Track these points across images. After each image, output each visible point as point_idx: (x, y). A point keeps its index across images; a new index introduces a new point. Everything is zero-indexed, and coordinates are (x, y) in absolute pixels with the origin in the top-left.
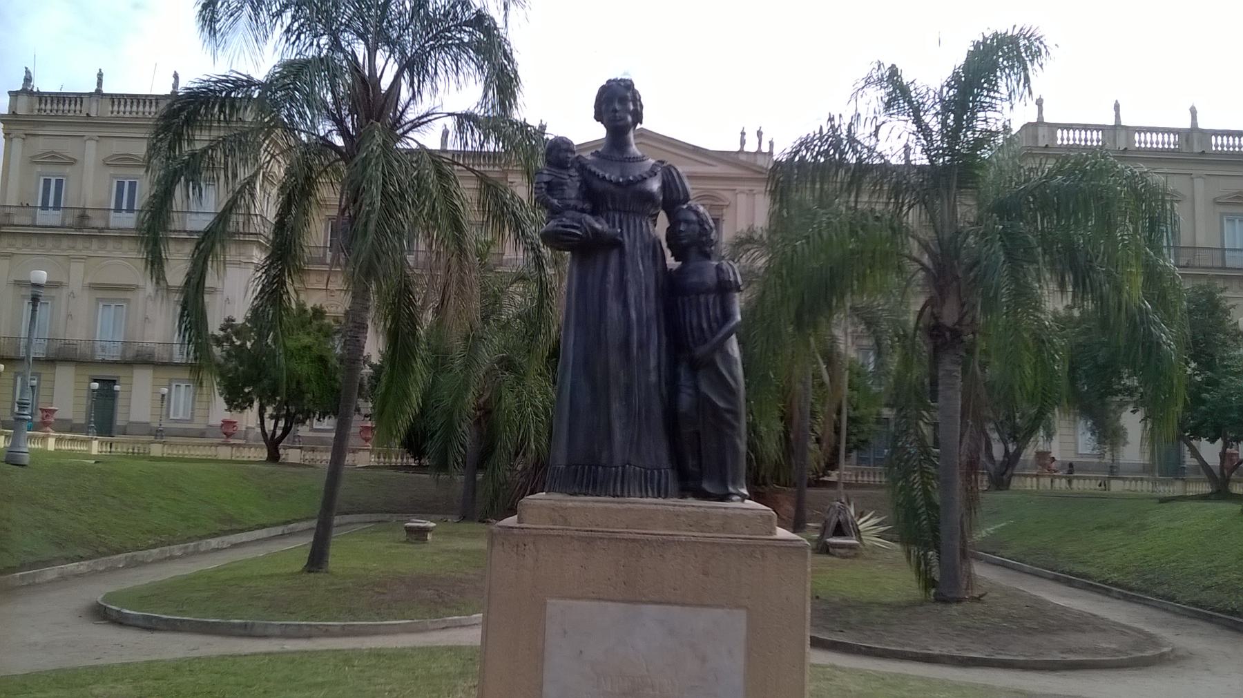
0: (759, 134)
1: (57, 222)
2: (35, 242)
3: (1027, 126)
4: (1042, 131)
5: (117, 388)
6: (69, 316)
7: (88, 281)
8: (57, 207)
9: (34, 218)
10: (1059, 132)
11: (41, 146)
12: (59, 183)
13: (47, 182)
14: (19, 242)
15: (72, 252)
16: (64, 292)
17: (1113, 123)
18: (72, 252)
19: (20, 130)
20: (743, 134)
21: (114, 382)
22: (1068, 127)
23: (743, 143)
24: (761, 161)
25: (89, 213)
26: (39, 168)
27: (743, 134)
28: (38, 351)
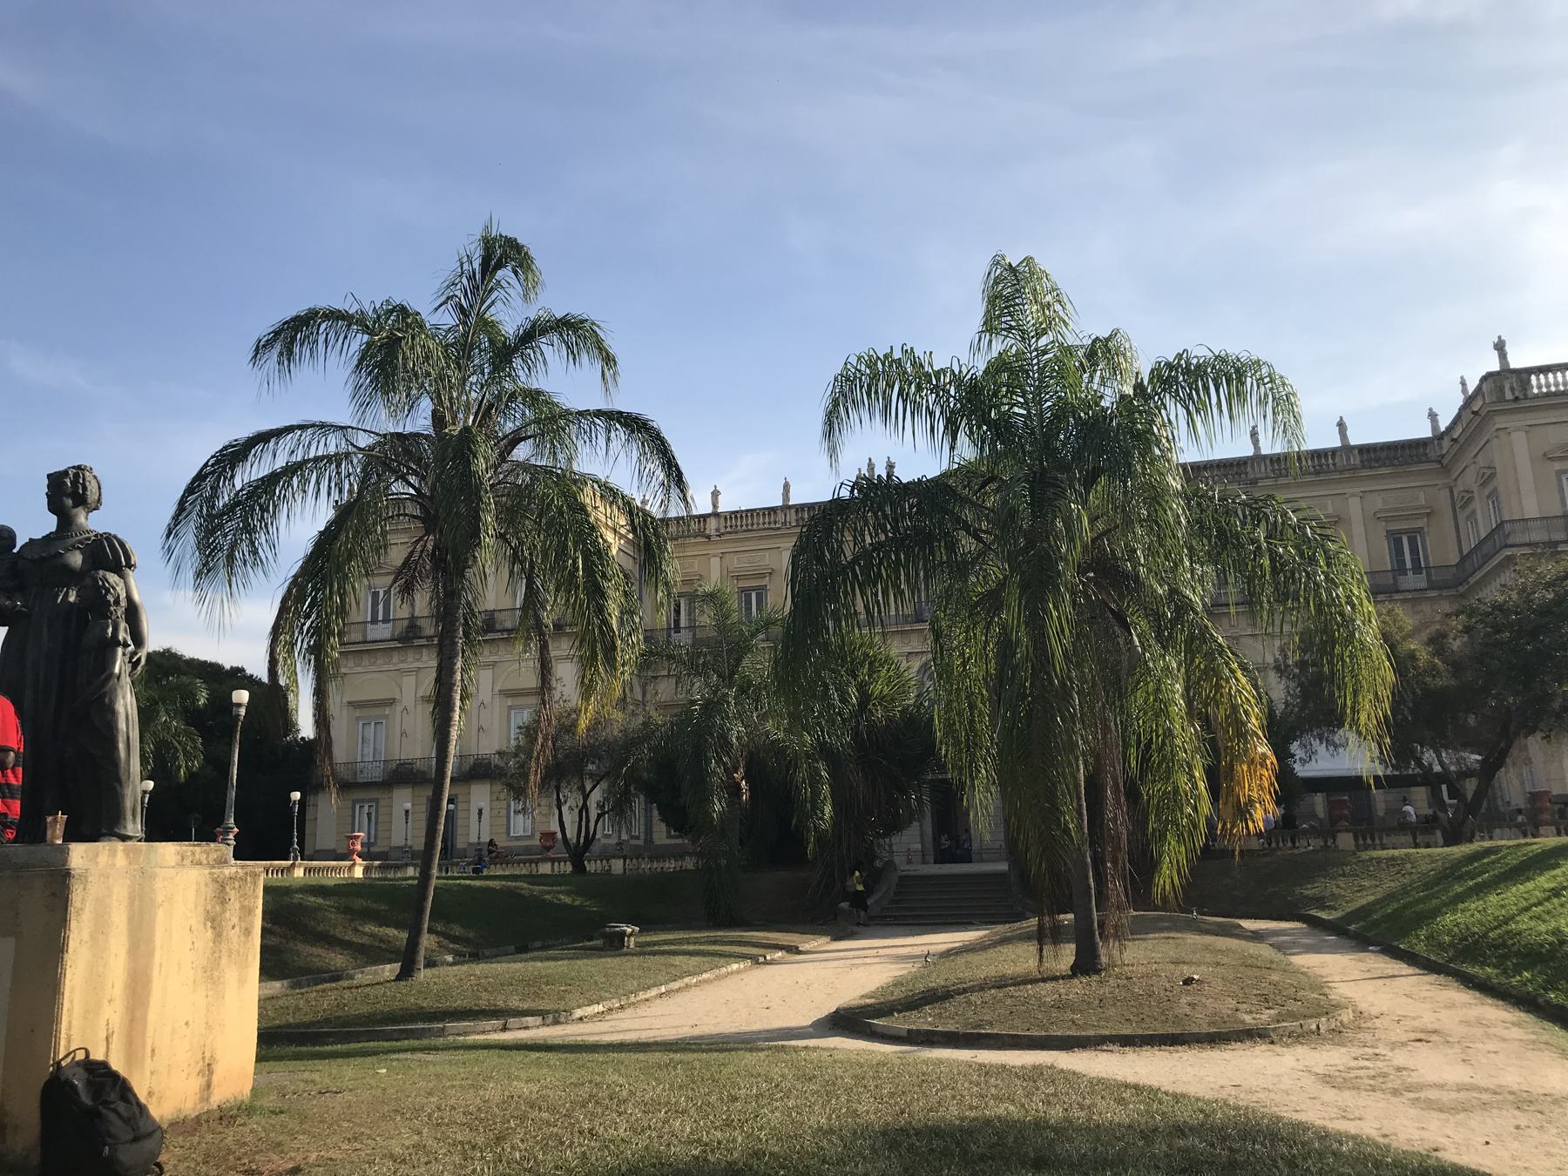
1: (387, 635)
2: (365, 657)
3: (1484, 379)
6: (403, 734)
7: (420, 694)
8: (386, 620)
9: (365, 635)
10: (1533, 378)
13: (375, 595)
15: (402, 666)
16: (399, 708)
18: (402, 666)
25: (420, 623)
28: (375, 773)
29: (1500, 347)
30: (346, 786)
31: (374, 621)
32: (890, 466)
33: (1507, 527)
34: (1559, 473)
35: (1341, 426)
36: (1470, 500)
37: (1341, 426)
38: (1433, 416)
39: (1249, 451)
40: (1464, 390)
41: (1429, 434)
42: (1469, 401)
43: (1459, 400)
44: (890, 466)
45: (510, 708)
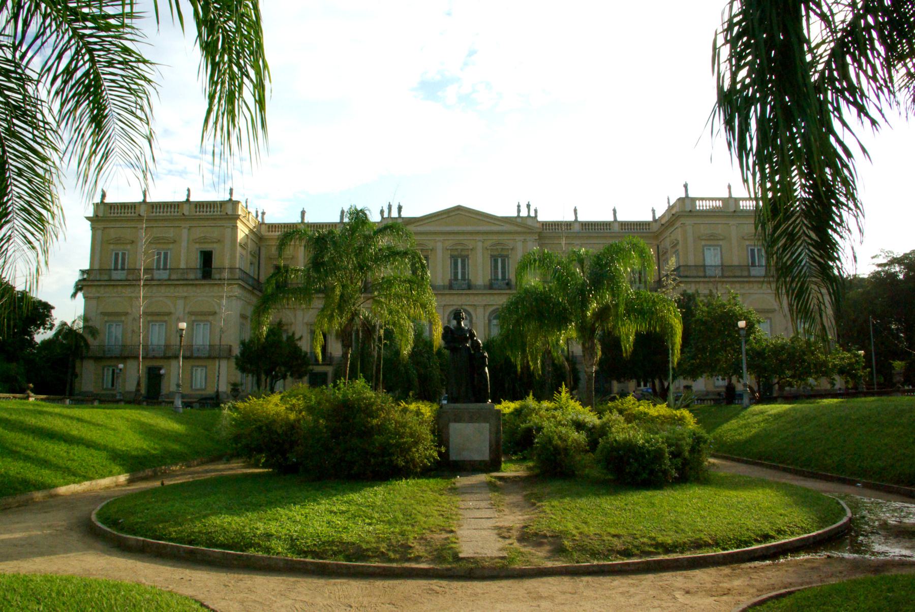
0: (528, 206)
3: (679, 199)
4: (687, 201)
5: (162, 372)
8: (123, 269)
9: (110, 276)
11: (113, 233)
12: (124, 254)
13: (117, 255)
14: (102, 290)
17: (727, 196)
19: (101, 225)
20: (519, 206)
21: (160, 369)
22: (702, 199)
23: (519, 211)
24: (529, 222)
26: (112, 247)
27: (519, 206)
29: (686, 186)
30: (97, 359)
31: (116, 269)
32: (400, 208)
33: (682, 269)
34: (704, 246)
35: (615, 211)
36: (665, 253)
37: (615, 211)
38: (653, 211)
39: (572, 219)
40: (669, 203)
41: (651, 219)
42: (671, 208)
43: (666, 207)
44: (400, 208)
45: (194, 321)
